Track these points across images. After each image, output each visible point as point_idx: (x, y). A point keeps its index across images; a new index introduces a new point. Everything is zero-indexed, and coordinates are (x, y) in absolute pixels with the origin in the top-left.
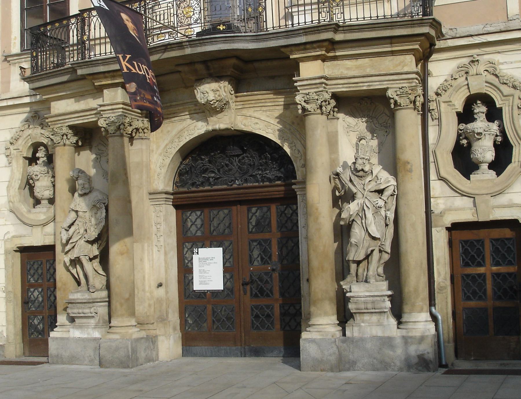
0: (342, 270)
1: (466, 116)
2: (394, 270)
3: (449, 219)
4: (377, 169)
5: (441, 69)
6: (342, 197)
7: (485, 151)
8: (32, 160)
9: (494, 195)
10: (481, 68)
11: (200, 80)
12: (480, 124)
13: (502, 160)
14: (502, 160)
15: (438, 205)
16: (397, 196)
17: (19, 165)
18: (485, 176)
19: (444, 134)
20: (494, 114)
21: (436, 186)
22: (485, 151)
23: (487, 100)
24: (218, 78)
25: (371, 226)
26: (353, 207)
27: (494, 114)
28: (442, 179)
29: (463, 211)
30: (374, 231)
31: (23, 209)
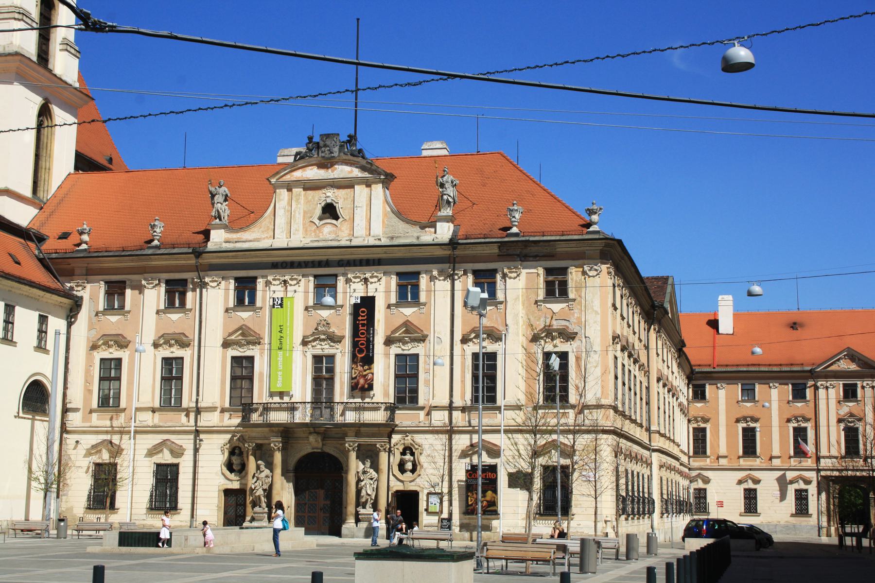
0: (358, 504)
1: (403, 453)
2: (375, 507)
3: (395, 489)
4: (372, 471)
5: (396, 438)
6: (359, 481)
7: (409, 466)
8: (232, 453)
9: (411, 482)
10: (409, 438)
11: (310, 433)
12: (408, 457)
13: (413, 471)
14: (413, 471)
15: (391, 484)
16: (378, 480)
17: (227, 454)
18: (409, 474)
19: (396, 459)
20: (413, 454)
21: (391, 476)
22: (409, 466)
23: (411, 449)
24: (318, 433)
25: (368, 489)
26: (363, 483)
27: (413, 454)
28: (394, 475)
29: (399, 487)
30: (369, 492)
31: (228, 472)
